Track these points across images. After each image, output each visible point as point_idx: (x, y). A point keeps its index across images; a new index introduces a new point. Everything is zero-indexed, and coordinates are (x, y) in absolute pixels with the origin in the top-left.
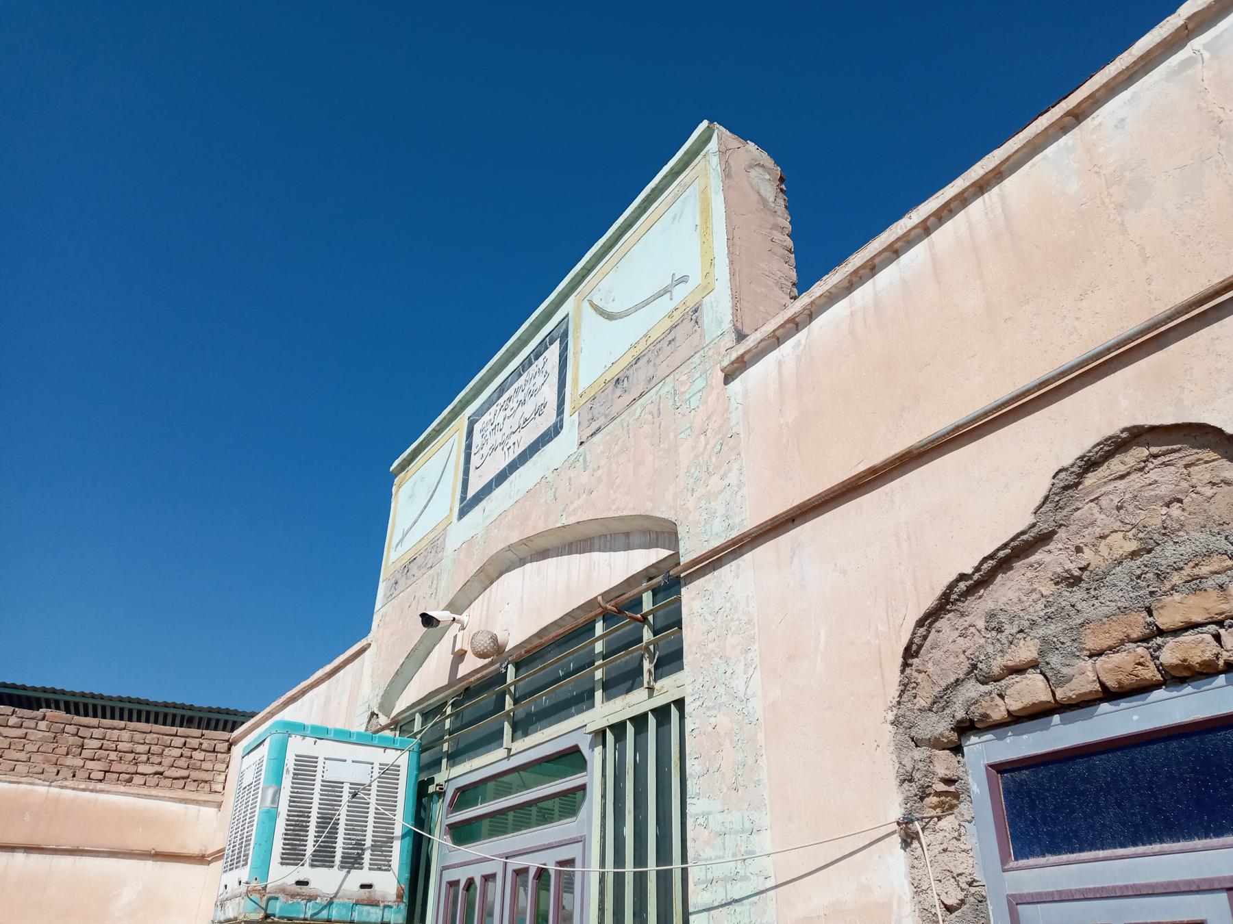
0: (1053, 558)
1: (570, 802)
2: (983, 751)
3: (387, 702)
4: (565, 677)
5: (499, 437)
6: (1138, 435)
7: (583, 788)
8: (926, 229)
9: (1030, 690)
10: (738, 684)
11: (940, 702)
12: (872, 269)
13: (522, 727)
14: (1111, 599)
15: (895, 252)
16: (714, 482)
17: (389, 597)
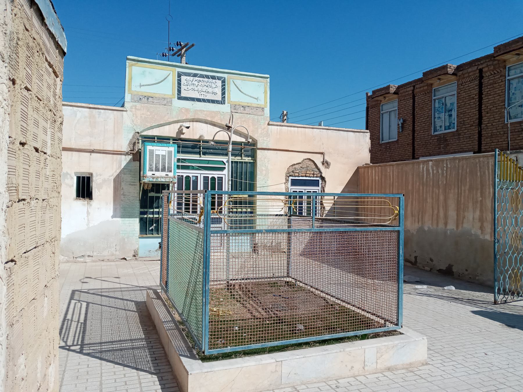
0: (301, 165)
1: (222, 169)
2: (291, 178)
3: (142, 132)
4: (218, 149)
5: (196, 89)
6: (309, 159)
7: (225, 168)
8: (298, 127)
9: (297, 174)
10: (267, 165)
11: (288, 173)
12: (291, 126)
13: (204, 154)
14: (304, 170)
15: (294, 127)
16: (265, 138)
17: (133, 100)
